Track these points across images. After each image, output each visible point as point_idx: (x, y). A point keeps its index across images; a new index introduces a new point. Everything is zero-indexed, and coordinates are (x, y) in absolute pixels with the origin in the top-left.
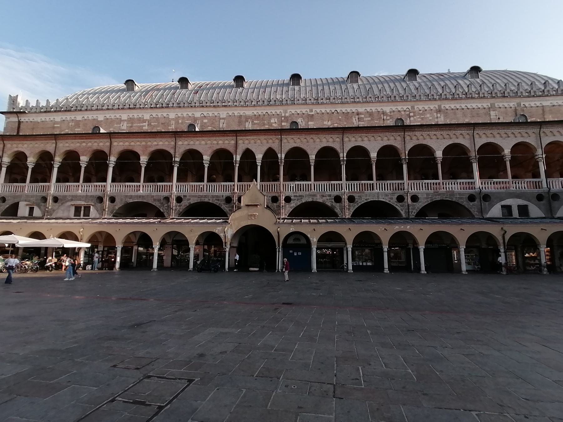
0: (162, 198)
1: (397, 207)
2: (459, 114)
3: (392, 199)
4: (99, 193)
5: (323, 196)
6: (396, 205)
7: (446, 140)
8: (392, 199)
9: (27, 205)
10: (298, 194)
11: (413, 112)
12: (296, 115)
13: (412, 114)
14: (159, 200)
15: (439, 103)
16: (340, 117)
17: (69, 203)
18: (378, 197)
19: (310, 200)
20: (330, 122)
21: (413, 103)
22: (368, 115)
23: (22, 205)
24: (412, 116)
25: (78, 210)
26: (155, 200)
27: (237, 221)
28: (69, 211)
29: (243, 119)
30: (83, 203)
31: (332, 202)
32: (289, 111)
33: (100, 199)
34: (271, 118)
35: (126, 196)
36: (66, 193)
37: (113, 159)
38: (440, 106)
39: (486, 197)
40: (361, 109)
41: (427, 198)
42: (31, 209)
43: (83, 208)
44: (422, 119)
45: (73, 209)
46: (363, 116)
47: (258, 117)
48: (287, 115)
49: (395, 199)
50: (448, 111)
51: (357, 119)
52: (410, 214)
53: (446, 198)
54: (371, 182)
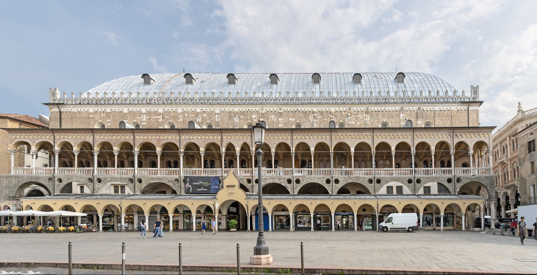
0: (174, 180)
3: (323, 181)
4: (130, 176)
5: (280, 179)
8: (323, 181)
9: (78, 185)
13: (349, 114)
14: (172, 182)
17: (109, 184)
21: (350, 106)
23: (74, 185)
25: (116, 187)
26: (169, 181)
27: (223, 196)
28: (110, 189)
30: (120, 183)
33: (131, 180)
35: (149, 178)
36: (106, 176)
37: (136, 150)
42: (82, 188)
43: (120, 187)
44: (356, 118)
45: (112, 188)
54: (311, 169)
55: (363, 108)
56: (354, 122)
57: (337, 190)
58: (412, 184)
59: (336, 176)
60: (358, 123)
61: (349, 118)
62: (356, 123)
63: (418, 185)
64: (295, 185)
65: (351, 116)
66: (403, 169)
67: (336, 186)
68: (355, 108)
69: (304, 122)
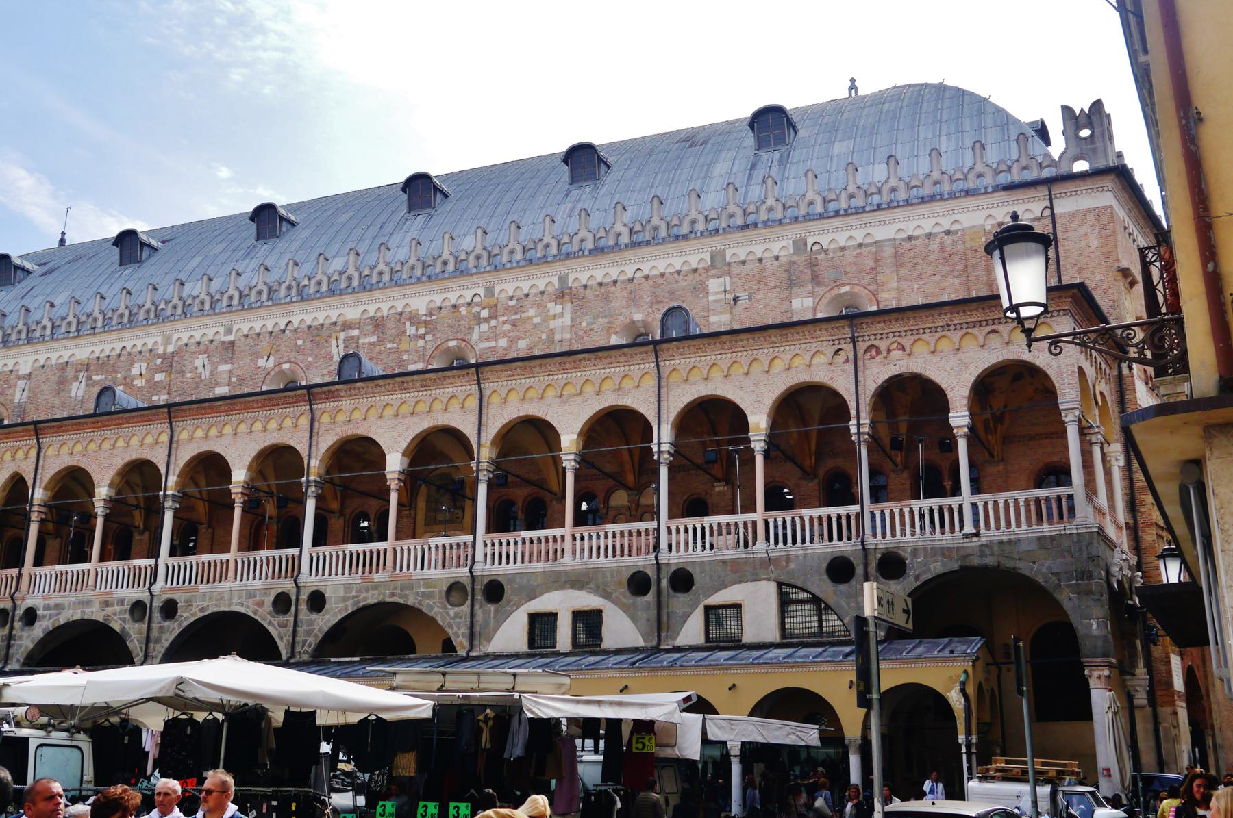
1: (270, 629)
2: (619, 297)
5: (107, 604)
6: (270, 623)
7: (416, 419)
8: (261, 604)
10: (52, 602)
11: (490, 307)
12: (192, 348)
13: (485, 313)
15: (559, 268)
16: (300, 342)
18: (231, 599)
19: (77, 617)
20: (272, 358)
22: (370, 328)
24: (487, 320)
29: (70, 373)
31: (124, 620)
32: (175, 337)
34: (132, 363)
38: (563, 280)
39: (495, 591)
40: (352, 314)
41: (345, 599)
46: (355, 332)
47: (102, 363)
48: (170, 349)
49: (268, 606)
50: (588, 291)
51: (341, 341)
52: (298, 649)
53: (393, 595)
55: (545, 279)
56: (503, 342)
57: (313, 641)
58: (650, 597)
59: (310, 581)
60: (522, 344)
61: (484, 327)
62: (512, 342)
63: (679, 601)
64: (155, 626)
65: (493, 316)
66: (610, 528)
67: (311, 623)
68: (509, 286)
69: (309, 365)
